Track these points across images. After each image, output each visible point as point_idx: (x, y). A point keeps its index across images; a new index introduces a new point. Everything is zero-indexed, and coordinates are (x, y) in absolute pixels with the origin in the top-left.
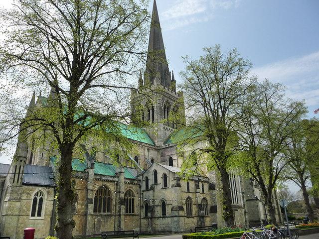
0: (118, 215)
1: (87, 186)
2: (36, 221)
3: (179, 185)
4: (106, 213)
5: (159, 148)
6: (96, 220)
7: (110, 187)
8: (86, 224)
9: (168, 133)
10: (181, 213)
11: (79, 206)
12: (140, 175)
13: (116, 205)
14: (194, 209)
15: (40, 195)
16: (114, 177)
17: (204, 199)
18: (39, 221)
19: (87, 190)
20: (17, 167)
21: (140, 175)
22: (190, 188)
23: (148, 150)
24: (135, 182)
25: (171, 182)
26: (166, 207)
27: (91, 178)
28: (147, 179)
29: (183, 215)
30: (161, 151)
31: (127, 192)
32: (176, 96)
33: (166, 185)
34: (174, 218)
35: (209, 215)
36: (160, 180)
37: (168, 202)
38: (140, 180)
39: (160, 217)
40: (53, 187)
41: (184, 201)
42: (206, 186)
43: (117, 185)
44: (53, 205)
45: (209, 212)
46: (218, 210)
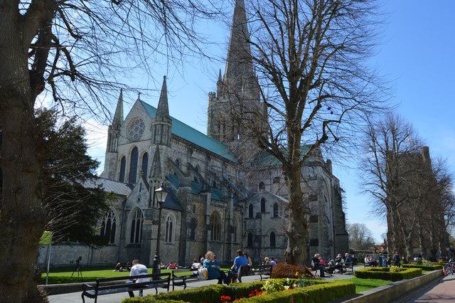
16: (225, 202)
19: (206, 216)
26: (277, 238)
28: (251, 207)
33: (276, 216)
36: (269, 208)
39: (268, 248)
43: (226, 211)
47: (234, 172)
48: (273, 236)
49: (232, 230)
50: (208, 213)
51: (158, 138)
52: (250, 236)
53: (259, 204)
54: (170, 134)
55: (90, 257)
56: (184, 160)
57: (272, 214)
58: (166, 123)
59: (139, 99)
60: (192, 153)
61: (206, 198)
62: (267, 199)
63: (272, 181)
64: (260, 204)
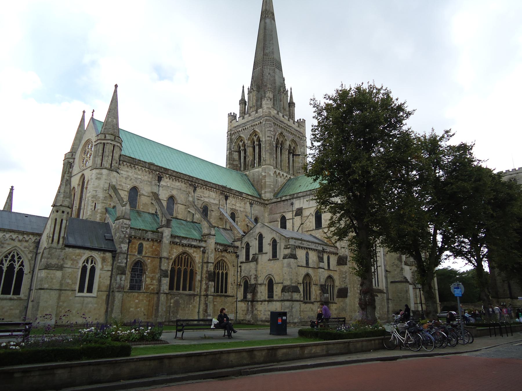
0: (204, 295)
1: (159, 253)
2: (85, 299)
3: (293, 256)
4: (187, 292)
5: (266, 202)
6: (172, 301)
7: (194, 255)
8: (158, 306)
9: (281, 181)
10: (296, 296)
11: (148, 281)
12: (238, 240)
13: (201, 281)
14: (315, 291)
15: (92, 263)
16: (201, 241)
17: (330, 277)
18: (90, 299)
19: (161, 258)
20: (57, 221)
21: (238, 240)
22: (310, 261)
23: (251, 204)
24: (230, 249)
25: (282, 252)
27: (166, 240)
28: (248, 246)
29: (298, 298)
30: (269, 207)
31: (218, 263)
32: (295, 126)
33: (274, 255)
34: (286, 302)
35: (336, 300)
36: (267, 248)
37: (277, 279)
38: (238, 247)
39: (265, 301)
41: (301, 280)
42: (334, 260)
43: (204, 252)
44: (111, 277)
45: (335, 296)
46: (349, 294)
48: (271, 284)
54: (116, 156)
56: (145, 189)
57: (270, 255)
60: (160, 179)
61: (162, 233)
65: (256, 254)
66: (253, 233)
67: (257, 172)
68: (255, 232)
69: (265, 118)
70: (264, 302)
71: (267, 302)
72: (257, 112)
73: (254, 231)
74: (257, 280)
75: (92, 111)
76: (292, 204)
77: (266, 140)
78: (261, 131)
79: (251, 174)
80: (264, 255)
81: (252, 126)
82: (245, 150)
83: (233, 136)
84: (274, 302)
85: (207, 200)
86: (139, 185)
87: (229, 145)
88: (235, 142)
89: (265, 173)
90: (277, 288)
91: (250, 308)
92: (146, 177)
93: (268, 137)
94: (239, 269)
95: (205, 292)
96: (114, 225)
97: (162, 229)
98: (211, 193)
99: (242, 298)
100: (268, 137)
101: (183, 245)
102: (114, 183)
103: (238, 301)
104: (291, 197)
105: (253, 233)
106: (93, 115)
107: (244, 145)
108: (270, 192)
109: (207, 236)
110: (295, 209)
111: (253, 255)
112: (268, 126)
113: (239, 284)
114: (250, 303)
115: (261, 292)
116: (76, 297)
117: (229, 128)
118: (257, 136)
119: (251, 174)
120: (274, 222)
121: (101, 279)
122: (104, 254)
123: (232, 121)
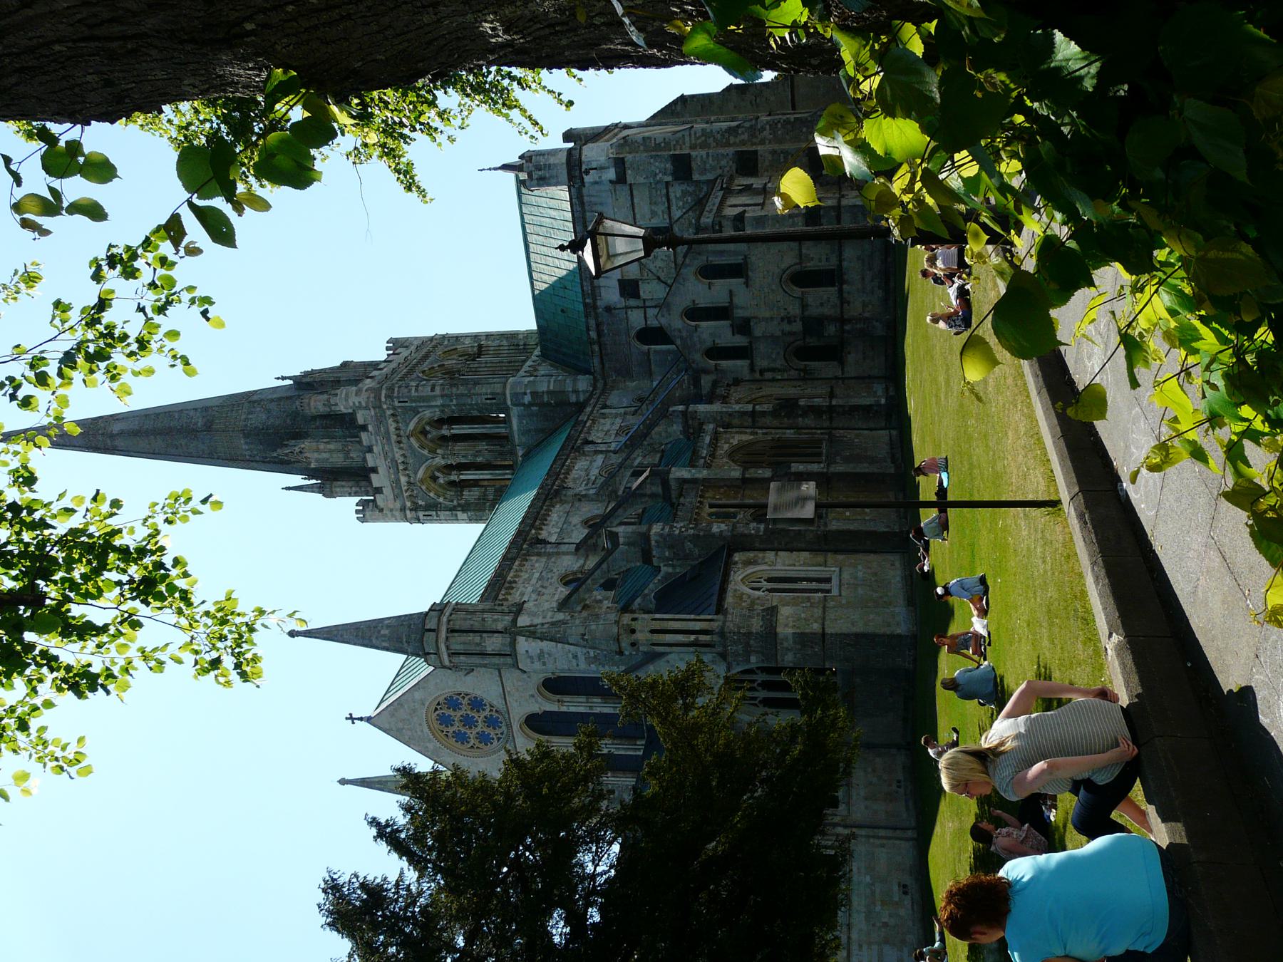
0: (831, 419)
5: (600, 385)
12: (696, 382)
18: (845, 576)
23: (605, 407)
26: (810, 265)
28: (716, 352)
33: (738, 270)
38: (715, 384)
39: (841, 291)
40: (730, 555)
43: (727, 426)
44: (791, 550)
47: (608, 421)
48: (803, 278)
49: (787, 407)
50: (736, 473)
51: (493, 643)
52: (805, 353)
53: (707, 326)
55: (889, 833)
56: (570, 563)
57: (735, 283)
58: (445, 619)
59: (369, 720)
61: (685, 481)
62: (687, 303)
63: (632, 302)
64: (703, 324)
65: (732, 326)
66: (681, 338)
67: (520, 422)
68: (680, 331)
69: (383, 399)
70: (845, 295)
71: (845, 286)
72: (364, 428)
73: (676, 333)
74: (795, 317)
75: (350, 721)
76: (609, 309)
77: (442, 396)
78: (415, 411)
79: (524, 440)
80: (736, 300)
81: (399, 442)
82: (461, 467)
83: (420, 502)
84: (845, 264)
85: (595, 472)
86: (557, 573)
87: (442, 514)
88: (435, 497)
89: (525, 394)
90: (812, 259)
91: (858, 326)
92: (537, 565)
93: (433, 390)
94: (768, 375)
95: (824, 417)
96: (664, 569)
97: (673, 485)
98: (576, 468)
99: (835, 363)
100: (433, 390)
101: (713, 455)
102: (555, 605)
103: (843, 373)
104: (593, 313)
105: (681, 338)
106: (361, 719)
107: (449, 468)
108: (575, 381)
109: (690, 422)
110: (623, 300)
111: (733, 335)
112: (406, 390)
113: (802, 374)
114: (847, 327)
115: (822, 304)
116: (840, 595)
117: (397, 514)
118: (428, 428)
119: (524, 440)
120: (649, 360)
121: (796, 564)
122: (736, 563)
123: (377, 506)
